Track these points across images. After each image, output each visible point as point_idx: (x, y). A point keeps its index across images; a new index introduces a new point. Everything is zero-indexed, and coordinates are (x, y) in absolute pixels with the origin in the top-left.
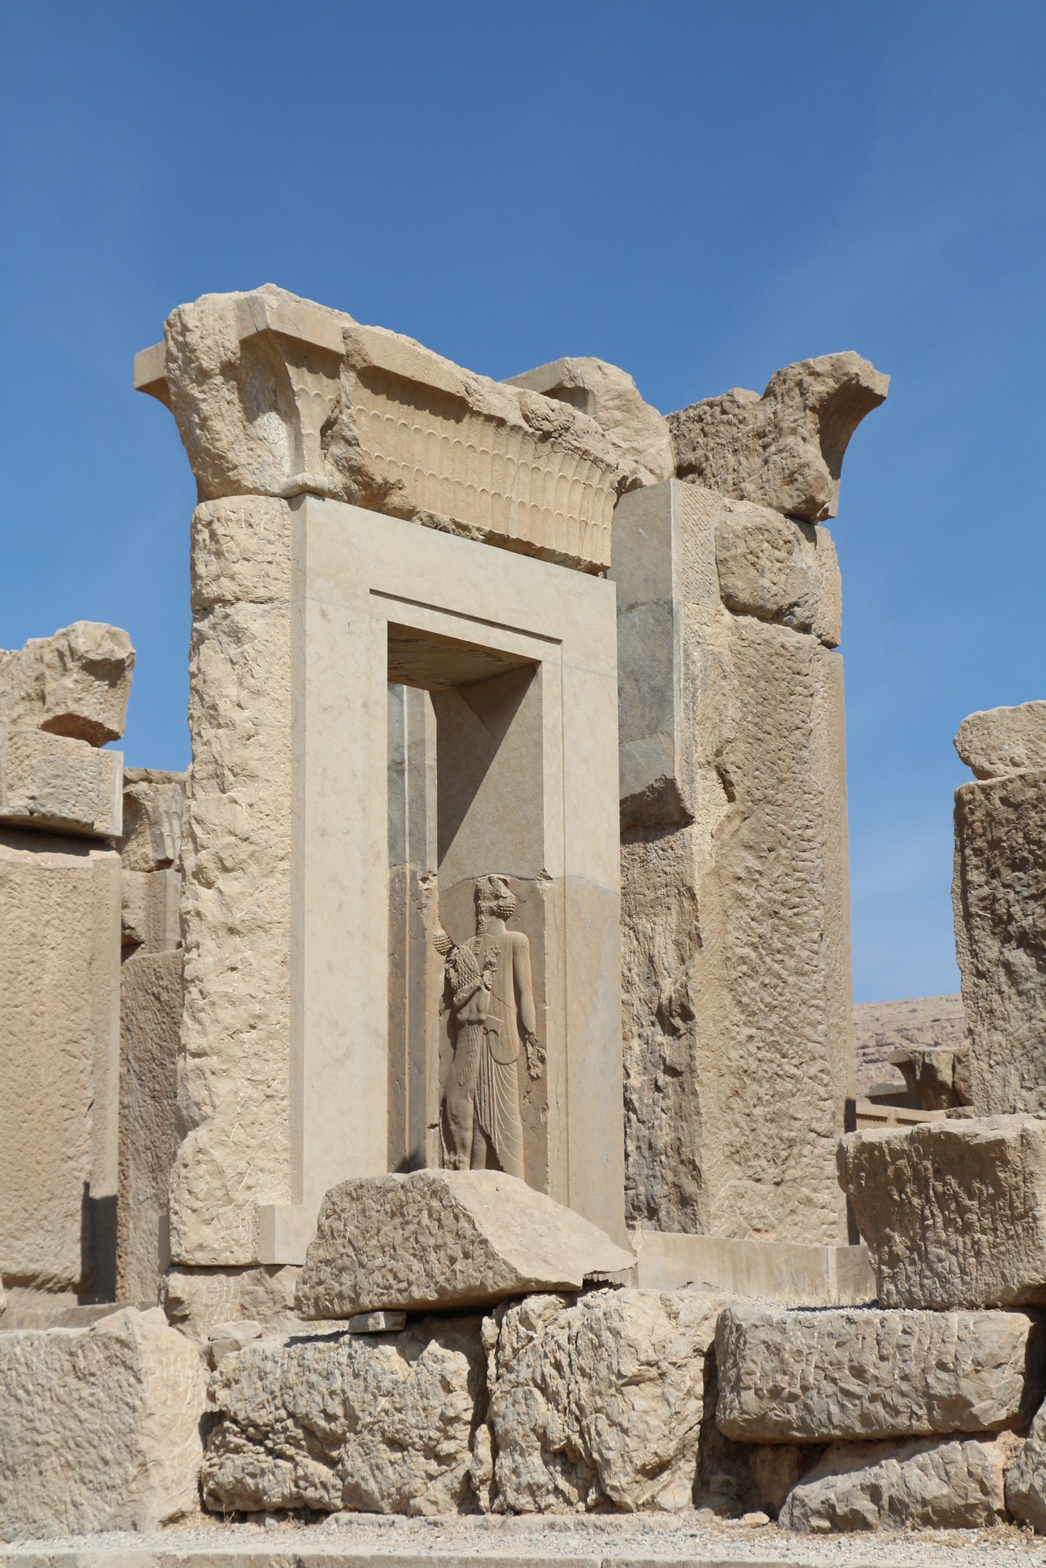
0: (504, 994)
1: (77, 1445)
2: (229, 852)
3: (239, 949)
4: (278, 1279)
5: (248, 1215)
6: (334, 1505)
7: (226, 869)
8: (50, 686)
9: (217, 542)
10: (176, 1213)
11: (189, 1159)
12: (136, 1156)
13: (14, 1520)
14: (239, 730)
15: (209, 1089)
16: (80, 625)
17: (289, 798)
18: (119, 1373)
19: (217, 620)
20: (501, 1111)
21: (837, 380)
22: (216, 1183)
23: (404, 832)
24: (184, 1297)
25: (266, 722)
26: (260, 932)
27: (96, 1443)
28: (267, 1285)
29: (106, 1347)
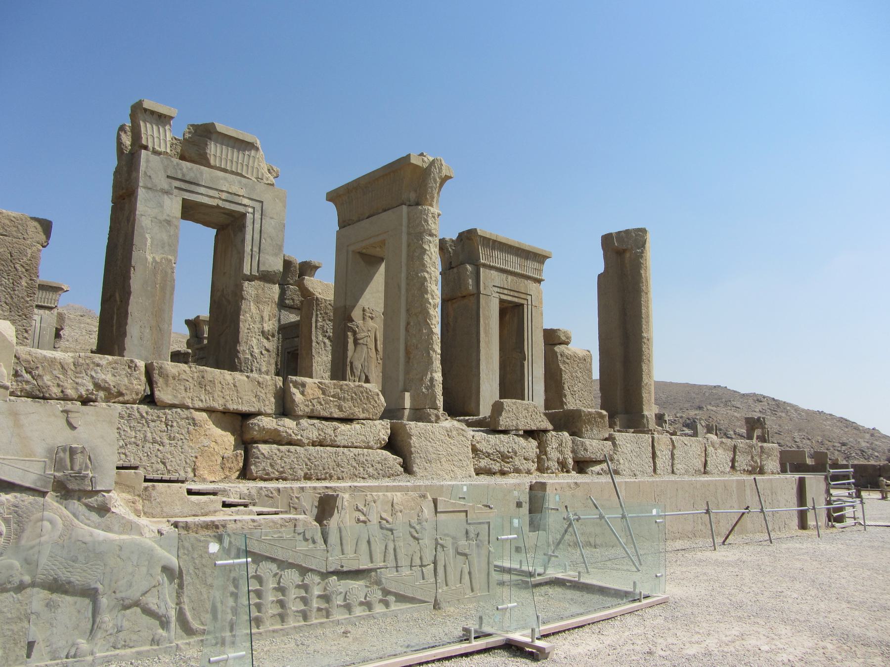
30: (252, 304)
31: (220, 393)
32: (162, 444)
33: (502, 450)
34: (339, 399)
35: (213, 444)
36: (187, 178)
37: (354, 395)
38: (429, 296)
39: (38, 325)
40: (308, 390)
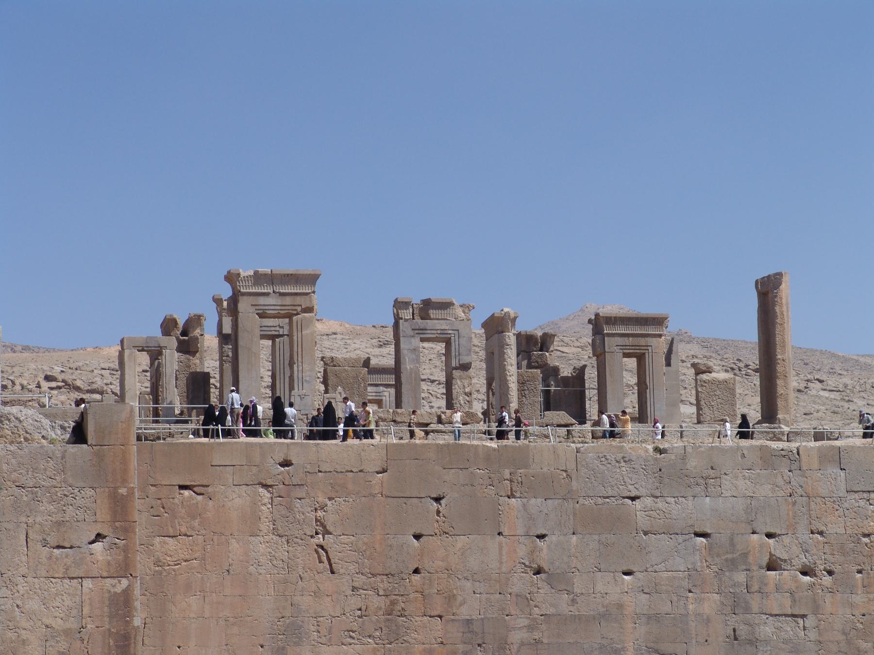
30: (458, 380)
32: (399, 433)
36: (421, 328)
38: (507, 372)
39: (388, 399)
40: (447, 414)
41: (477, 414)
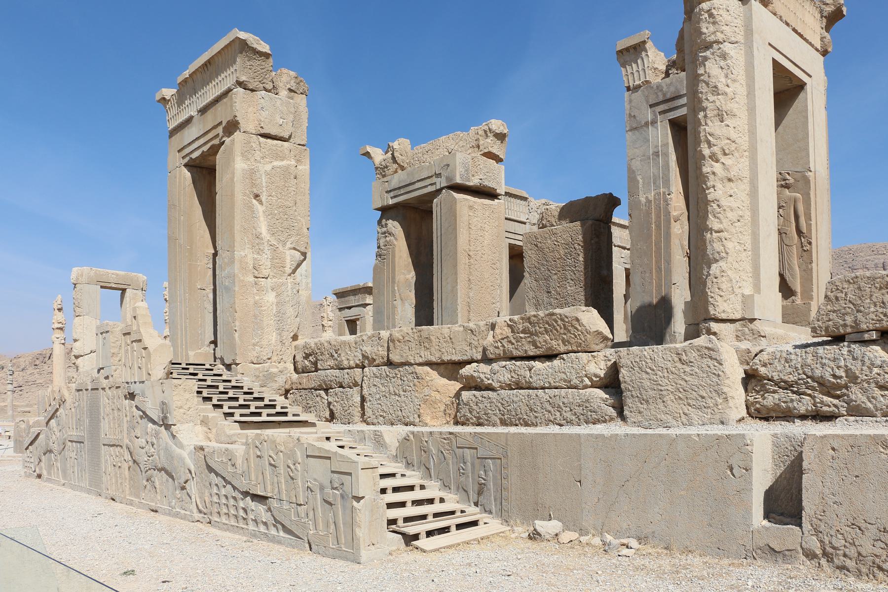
0: (790, 218)
1: (685, 391)
2: (728, 147)
3: (731, 187)
4: (754, 325)
5: (740, 298)
6: (842, 413)
7: (725, 154)
8: (481, 142)
9: (714, 18)
10: (712, 297)
11: (718, 273)
12: (529, 301)
13: (649, 420)
14: (729, 95)
15: (723, 246)
16: (493, 121)
17: (747, 126)
18: (708, 361)
19: (715, 51)
20: (789, 264)
21: (835, 6)
22: (729, 285)
23: (660, 178)
24: (718, 332)
25: (738, 93)
26: (739, 181)
27: (696, 390)
28: (749, 327)
29: (698, 350)
31: (437, 347)
33: (818, 373)
34: (532, 334)
35: (433, 394)
37: (547, 326)
41: (577, 320)
